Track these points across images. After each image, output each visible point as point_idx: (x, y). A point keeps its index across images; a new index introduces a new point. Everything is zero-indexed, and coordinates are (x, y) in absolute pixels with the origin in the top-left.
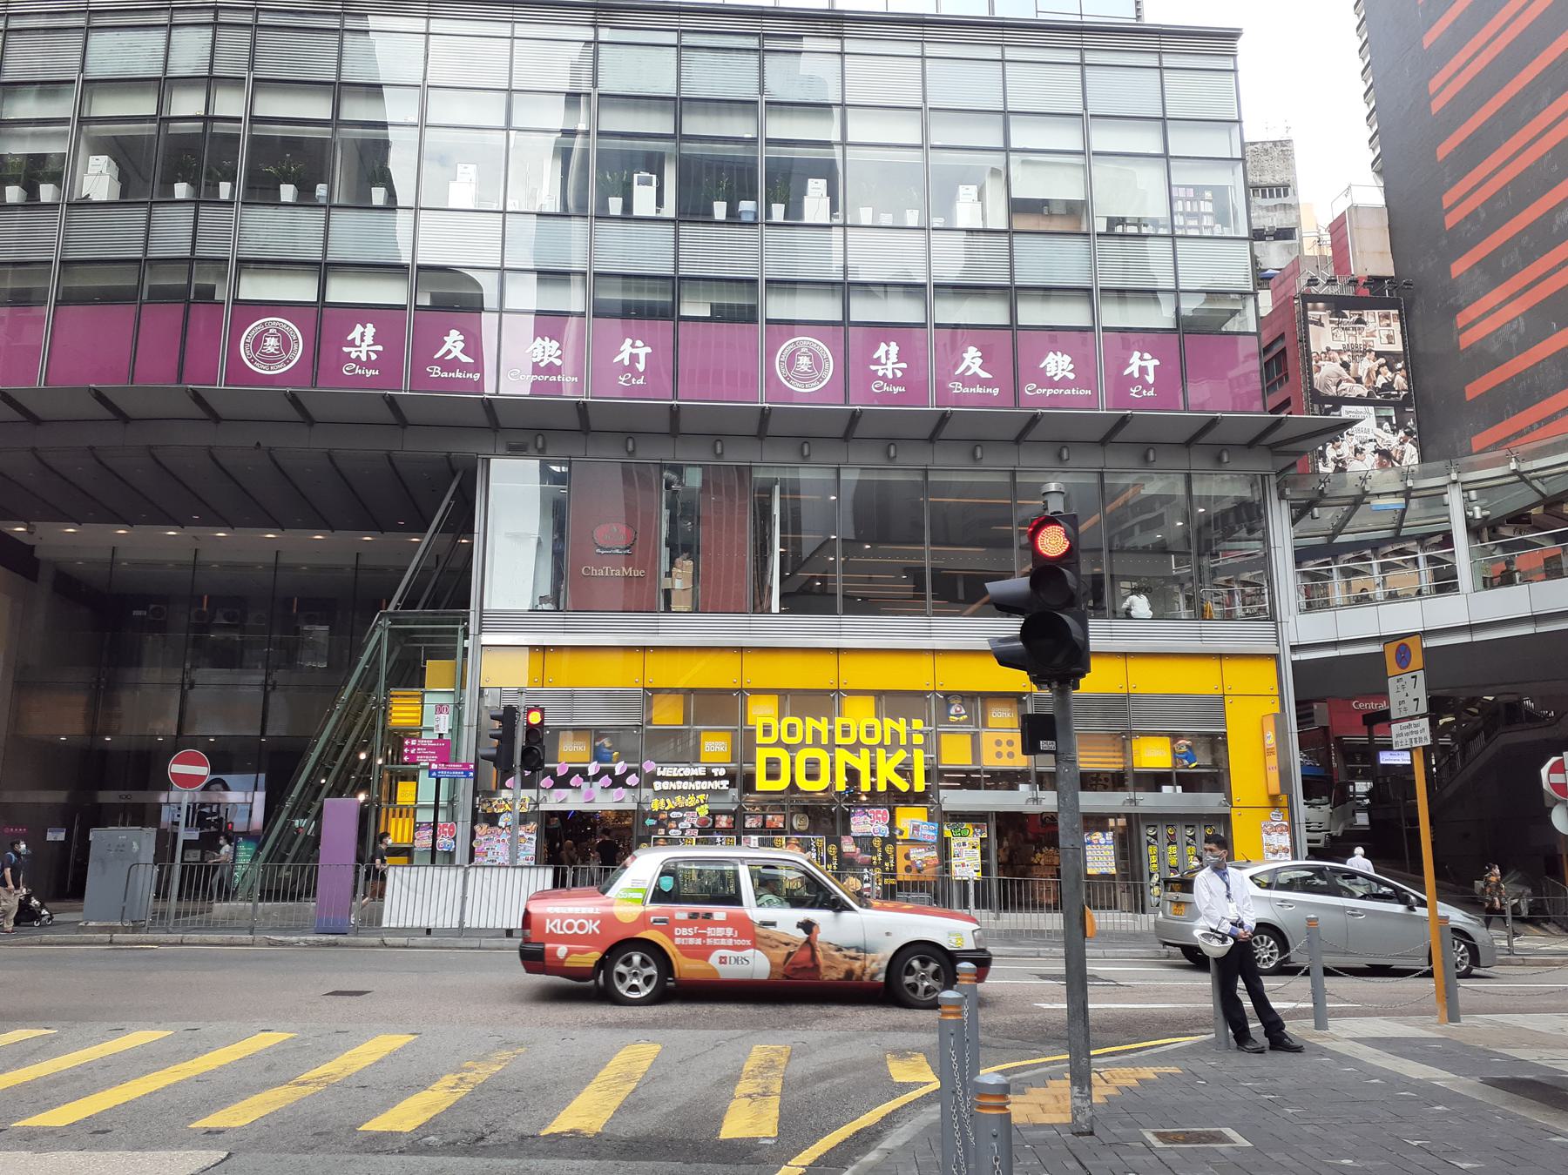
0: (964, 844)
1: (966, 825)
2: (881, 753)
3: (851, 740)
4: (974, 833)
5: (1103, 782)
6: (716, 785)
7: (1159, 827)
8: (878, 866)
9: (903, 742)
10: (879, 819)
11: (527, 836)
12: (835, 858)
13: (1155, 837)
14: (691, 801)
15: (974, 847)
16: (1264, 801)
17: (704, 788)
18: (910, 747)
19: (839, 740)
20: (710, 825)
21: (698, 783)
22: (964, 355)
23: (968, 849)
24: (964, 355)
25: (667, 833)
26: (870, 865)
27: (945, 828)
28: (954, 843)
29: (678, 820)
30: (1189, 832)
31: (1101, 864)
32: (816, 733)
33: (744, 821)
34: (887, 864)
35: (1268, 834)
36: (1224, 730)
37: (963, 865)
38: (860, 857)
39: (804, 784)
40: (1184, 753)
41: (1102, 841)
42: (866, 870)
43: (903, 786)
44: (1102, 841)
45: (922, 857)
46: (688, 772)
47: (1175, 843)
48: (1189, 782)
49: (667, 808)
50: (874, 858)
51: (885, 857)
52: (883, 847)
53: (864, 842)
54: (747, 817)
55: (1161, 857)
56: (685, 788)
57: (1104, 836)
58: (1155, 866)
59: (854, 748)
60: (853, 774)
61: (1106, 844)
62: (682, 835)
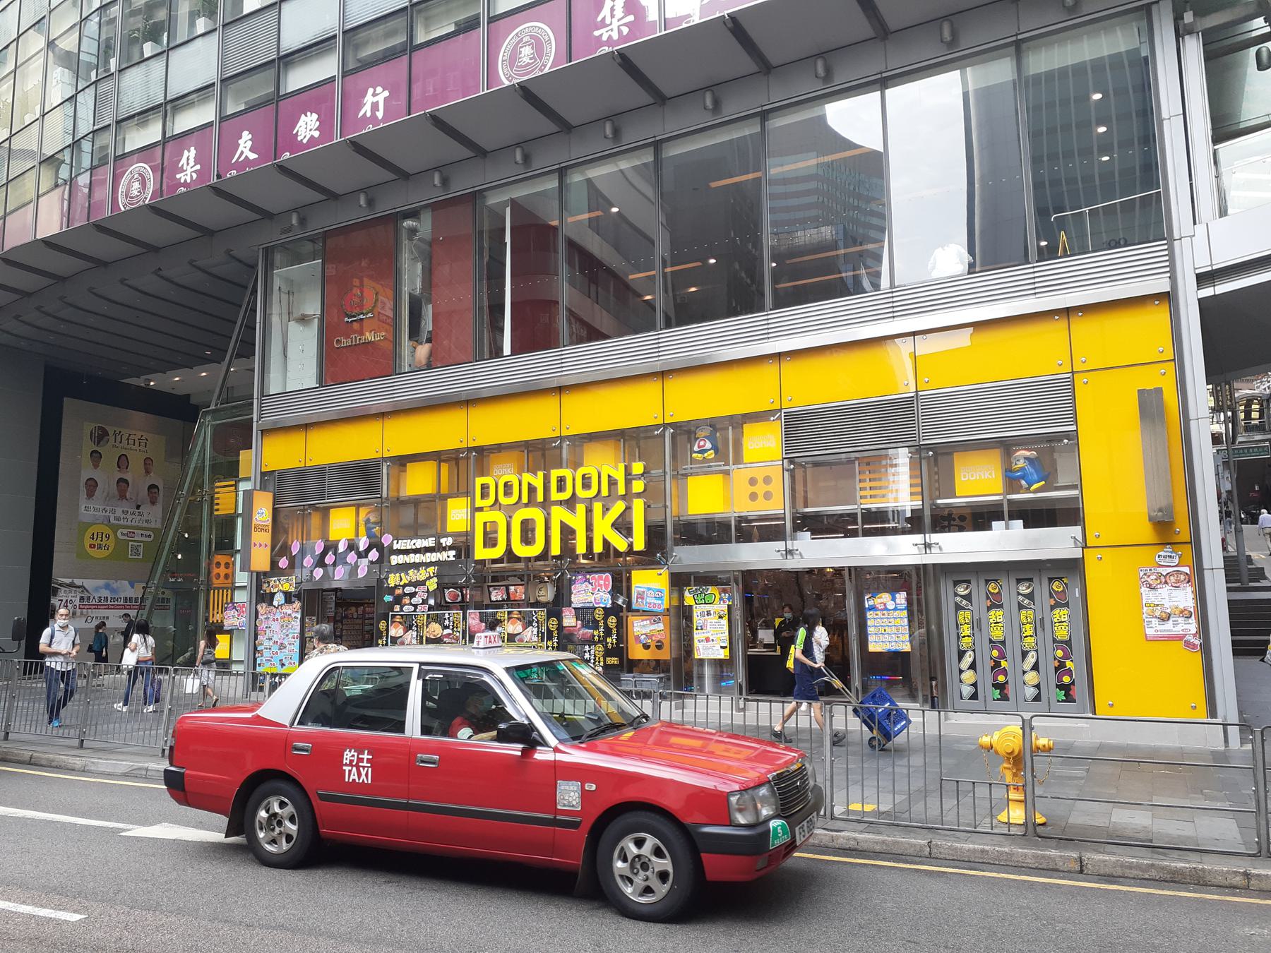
0: (709, 613)
1: (711, 589)
2: (598, 507)
3: (566, 495)
4: (721, 599)
5: (957, 522)
6: (442, 556)
7: (974, 583)
8: (600, 642)
9: (621, 490)
10: (600, 585)
11: (293, 615)
12: (555, 634)
13: (968, 598)
14: (422, 575)
15: (720, 617)
16: (1146, 533)
17: (434, 560)
18: (628, 497)
19: (555, 496)
20: (460, 599)
21: (428, 554)
23: (713, 619)
25: (402, 610)
26: (591, 642)
27: (687, 594)
28: (697, 611)
29: (412, 595)
30: (1024, 589)
31: (888, 638)
32: (532, 490)
33: (490, 593)
34: (609, 640)
35: (1150, 587)
36: (1074, 428)
37: (708, 640)
38: (581, 632)
39: (521, 550)
40: (1022, 469)
41: (891, 605)
42: (587, 648)
43: (620, 544)
44: (891, 605)
45: (647, 630)
46: (420, 543)
47: (1001, 606)
48: (1037, 516)
49: (401, 584)
50: (596, 633)
51: (608, 632)
52: (605, 618)
53: (585, 614)
54: (491, 589)
55: (977, 625)
56: (417, 561)
57: (894, 599)
58: (1030, 640)
59: (570, 504)
60: (567, 532)
61: (895, 609)
62: (415, 611)
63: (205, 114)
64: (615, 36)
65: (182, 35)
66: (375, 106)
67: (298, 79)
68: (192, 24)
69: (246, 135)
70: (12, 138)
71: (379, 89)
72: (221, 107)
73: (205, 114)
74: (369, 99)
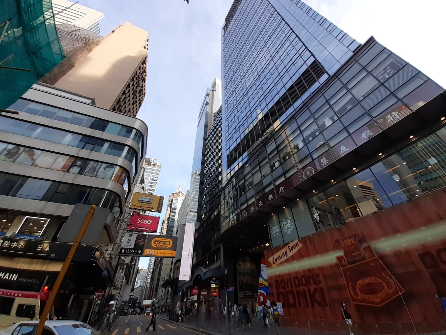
22: (341, 149)
24: (341, 149)
63: (253, 200)
64: (326, 164)
65: (248, 189)
66: (282, 190)
67: (267, 190)
68: (249, 188)
69: (260, 201)
70: (263, 180)
71: (282, 187)
72: (255, 198)
73: (253, 200)
74: (280, 189)
